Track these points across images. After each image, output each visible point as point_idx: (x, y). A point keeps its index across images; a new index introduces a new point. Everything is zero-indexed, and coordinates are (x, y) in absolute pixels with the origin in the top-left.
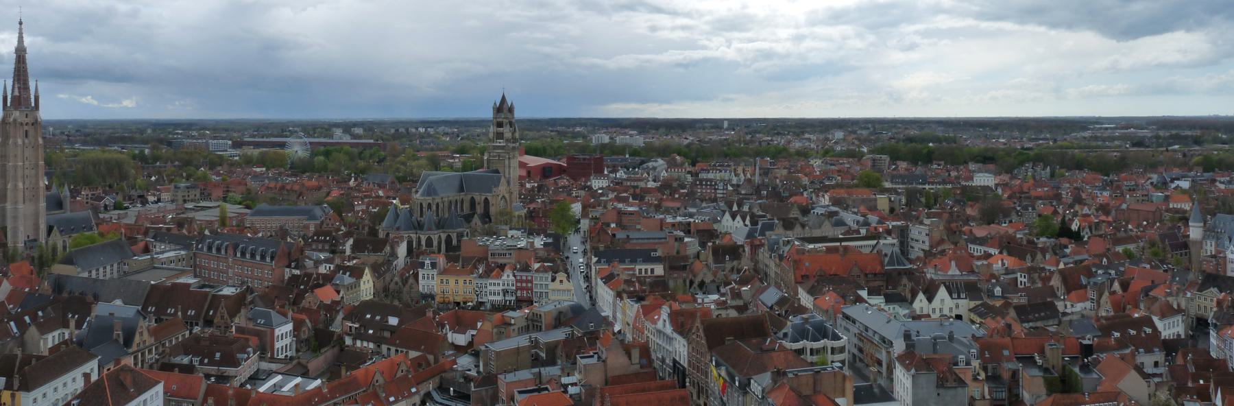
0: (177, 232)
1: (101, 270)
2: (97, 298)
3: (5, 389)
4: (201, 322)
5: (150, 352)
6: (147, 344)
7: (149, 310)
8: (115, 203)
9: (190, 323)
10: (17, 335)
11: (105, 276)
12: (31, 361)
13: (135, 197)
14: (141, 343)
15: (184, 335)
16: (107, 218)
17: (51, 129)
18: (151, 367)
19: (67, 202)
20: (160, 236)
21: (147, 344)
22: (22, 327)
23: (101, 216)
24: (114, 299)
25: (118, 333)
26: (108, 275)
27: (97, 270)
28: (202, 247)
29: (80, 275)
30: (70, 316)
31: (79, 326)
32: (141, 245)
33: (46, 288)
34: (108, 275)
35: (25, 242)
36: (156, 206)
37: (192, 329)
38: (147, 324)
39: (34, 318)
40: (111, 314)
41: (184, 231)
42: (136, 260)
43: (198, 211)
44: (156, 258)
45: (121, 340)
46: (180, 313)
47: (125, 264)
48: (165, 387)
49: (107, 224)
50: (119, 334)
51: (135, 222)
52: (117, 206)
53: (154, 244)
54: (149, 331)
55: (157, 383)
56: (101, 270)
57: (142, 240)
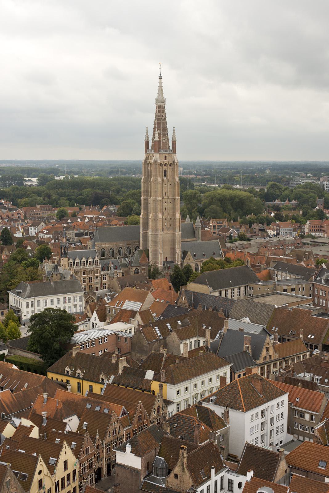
0: (297, 264)
1: (230, 291)
2: (227, 315)
3: (154, 379)
4: (320, 346)
5: (275, 365)
6: (272, 359)
7: (273, 330)
8: (238, 235)
9: (312, 347)
10: (160, 337)
11: (233, 296)
12: (175, 360)
13: (257, 230)
14: (268, 357)
15: (305, 356)
16: (234, 247)
17: (181, 169)
18: (277, 379)
19: (199, 232)
20: (281, 266)
21: (272, 359)
22: (164, 330)
23: (228, 245)
24: (242, 317)
25: (247, 346)
26: (236, 298)
27: (227, 291)
28: (321, 279)
29: (212, 294)
30: (205, 327)
31: (213, 337)
32: (264, 272)
33: (183, 302)
34: (236, 298)
35: (164, 262)
36: (276, 239)
37: (313, 351)
38: (272, 341)
39: (174, 326)
40: (241, 330)
41: (303, 263)
42: (259, 285)
43: (315, 246)
44: (278, 285)
45: (250, 352)
46: (301, 336)
47: (250, 288)
48: (289, 396)
49: (233, 253)
50: (248, 348)
51: (258, 252)
52: (242, 238)
53: (276, 272)
54: (274, 348)
55: (282, 393)
56: (230, 291)
57: (265, 269)
